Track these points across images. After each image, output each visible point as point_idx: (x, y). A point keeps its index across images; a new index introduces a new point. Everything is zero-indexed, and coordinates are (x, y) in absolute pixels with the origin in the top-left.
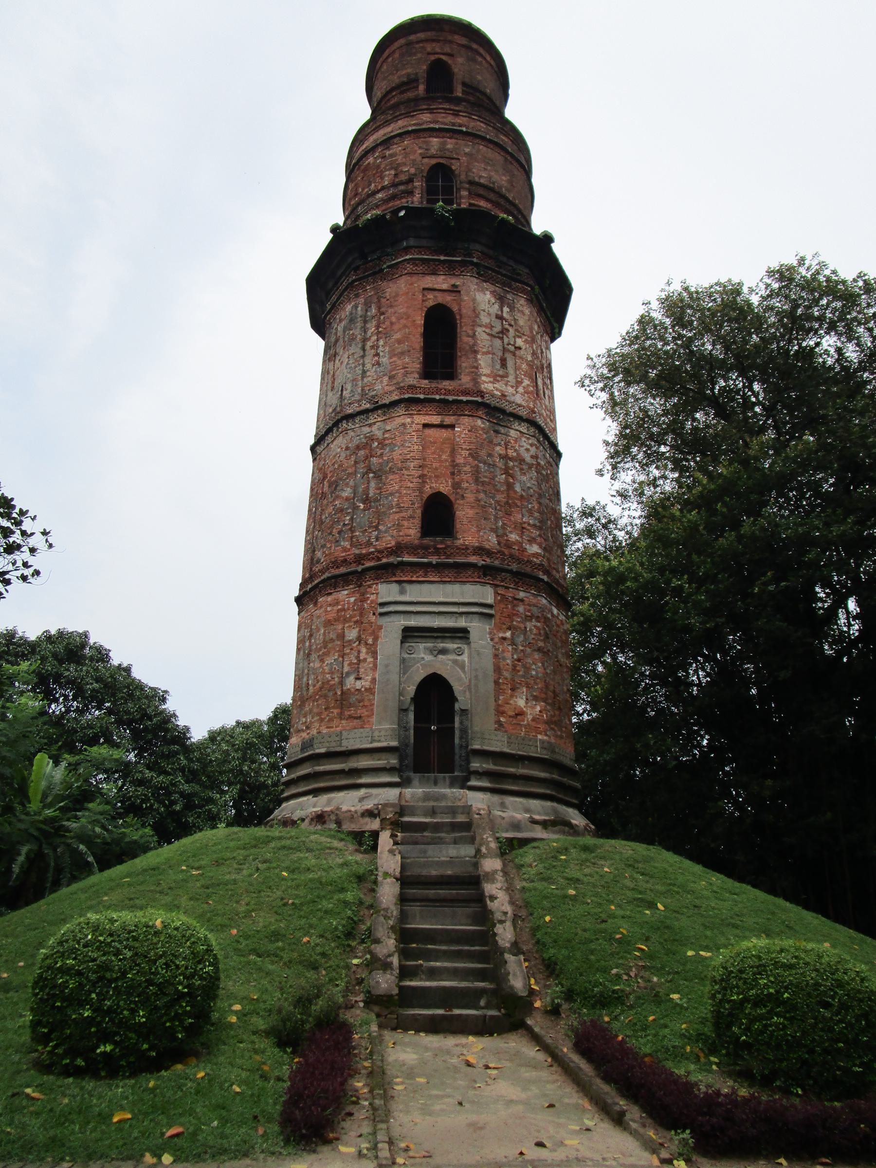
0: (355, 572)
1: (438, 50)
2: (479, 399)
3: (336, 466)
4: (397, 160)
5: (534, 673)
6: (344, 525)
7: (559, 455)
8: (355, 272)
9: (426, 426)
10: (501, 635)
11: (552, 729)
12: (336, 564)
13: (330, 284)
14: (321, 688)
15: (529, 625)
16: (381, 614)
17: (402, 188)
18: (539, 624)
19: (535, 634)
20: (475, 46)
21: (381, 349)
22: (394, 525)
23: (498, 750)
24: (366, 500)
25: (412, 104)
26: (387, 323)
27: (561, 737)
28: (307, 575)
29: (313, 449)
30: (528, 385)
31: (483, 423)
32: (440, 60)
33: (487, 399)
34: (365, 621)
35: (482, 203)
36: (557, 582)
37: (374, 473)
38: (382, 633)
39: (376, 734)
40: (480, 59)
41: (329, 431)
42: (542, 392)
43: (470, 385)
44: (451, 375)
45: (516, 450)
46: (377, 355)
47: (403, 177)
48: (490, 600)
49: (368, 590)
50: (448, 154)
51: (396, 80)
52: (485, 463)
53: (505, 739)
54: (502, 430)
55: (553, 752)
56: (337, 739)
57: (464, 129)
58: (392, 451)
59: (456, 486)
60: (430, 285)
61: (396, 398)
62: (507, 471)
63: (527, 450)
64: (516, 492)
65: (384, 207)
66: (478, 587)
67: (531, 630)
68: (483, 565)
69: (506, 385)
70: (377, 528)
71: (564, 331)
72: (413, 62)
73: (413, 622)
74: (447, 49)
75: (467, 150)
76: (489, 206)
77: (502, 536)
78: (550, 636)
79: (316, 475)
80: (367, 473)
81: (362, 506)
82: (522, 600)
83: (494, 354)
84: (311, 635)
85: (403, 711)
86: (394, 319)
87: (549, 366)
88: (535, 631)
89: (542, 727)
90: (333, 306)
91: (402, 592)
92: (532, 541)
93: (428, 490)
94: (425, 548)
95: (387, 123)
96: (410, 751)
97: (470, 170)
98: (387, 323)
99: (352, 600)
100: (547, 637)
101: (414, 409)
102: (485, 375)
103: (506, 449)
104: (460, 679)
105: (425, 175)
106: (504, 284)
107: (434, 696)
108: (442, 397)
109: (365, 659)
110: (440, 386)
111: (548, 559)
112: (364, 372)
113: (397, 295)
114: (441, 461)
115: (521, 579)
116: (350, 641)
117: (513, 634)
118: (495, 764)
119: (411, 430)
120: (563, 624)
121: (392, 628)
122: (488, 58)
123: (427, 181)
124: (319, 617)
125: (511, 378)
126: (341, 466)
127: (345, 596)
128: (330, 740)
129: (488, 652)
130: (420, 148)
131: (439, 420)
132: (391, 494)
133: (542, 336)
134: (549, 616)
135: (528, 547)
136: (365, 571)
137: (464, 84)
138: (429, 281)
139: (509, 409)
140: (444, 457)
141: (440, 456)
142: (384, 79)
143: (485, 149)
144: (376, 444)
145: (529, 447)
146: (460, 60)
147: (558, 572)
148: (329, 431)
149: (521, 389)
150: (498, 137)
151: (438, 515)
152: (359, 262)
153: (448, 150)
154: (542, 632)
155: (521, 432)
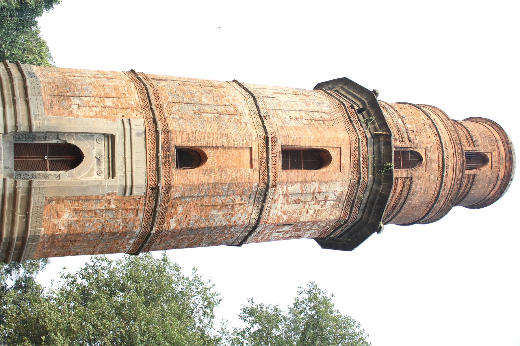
0: (151, 105)
1: (494, 159)
2: (270, 184)
3: (222, 94)
4: (423, 132)
5: (87, 225)
6: (183, 98)
7: (240, 245)
8: (350, 106)
9: (251, 149)
10: (112, 201)
11: (49, 240)
12: (156, 92)
13: (343, 92)
14: (71, 83)
15: (120, 220)
16: (123, 120)
17: (405, 135)
18: (121, 228)
19: (114, 225)
20: (499, 183)
21: (300, 121)
22: (183, 128)
23: (32, 200)
24: (200, 112)
25: (459, 142)
26: (317, 125)
27: (43, 247)
28: (149, 77)
29: (235, 81)
30: (283, 219)
31: (255, 187)
32: (488, 160)
33: (271, 190)
34: (118, 110)
35: (399, 187)
36: (152, 243)
37: (218, 117)
38: (109, 121)
39: (40, 117)
40: (491, 186)
41: (247, 90)
42: (280, 230)
43: (279, 179)
44: (285, 167)
45: (239, 210)
46: (297, 119)
47: (412, 136)
48: (135, 192)
49: (139, 113)
50: (428, 164)
51: (475, 133)
52: (228, 189)
53: (40, 205)
54: (252, 200)
55: (33, 240)
56: (37, 93)
57: (445, 175)
58: (233, 128)
59: (212, 170)
60: (342, 153)
61: (268, 131)
62: (224, 205)
63: (240, 218)
64: (210, 210)
65: (392, 124)
66: (144, 183)
67: (117, 222)
68: (159, 187)
69: (282, 203)
70: (182, 118)
71: (325, 249)
72: (486, 143)
73: (119, 142)
74: (495, 165)
75: (432, 177)
76: (398, 192)
78: (114, 237)
79: (217, 83)
80: (218, 113)
81: (196, 109)
82: (137, 215)
83: (302, 194)
84: (108, 78)
85: (58, 134)
86: (320, 129)
87: (300, 237)
88: (116, 225)
89: (50, 232)
90: (329, 94)
91: (138, 134)
92: (178, 222)
93: (207, 152)
94: (169, 149)
95: (446, 126)
96: (29, 141)
97: (419, 179)
98: (317, 125)
99: (132, 103)
100: (113, 234)
101: (263, 142)
102: (287, 188)
104: (80, 174)
105: (415, 150)
106: (348, 201)
107: (69, 156)
108: (270, 160)
109: (92, 111)
110: (277, 158)
111: (167, 235)
112: (285, 111)
113: (335, 131)
114: (228, 159)
115: (151, 215)
116: (104, 101)
117: (113, 210)
118: (21, 198)
119: (248, 140)
120: (123, 248)
121: (113, 127)
122: (493, 192)
123: (411, 151)
124: (120, 82)
125: (286, 207)
126: (223, 97)
127: (135, 98)
128: (36, 88)
129: (100, 192)
130: (431, 147)
131: (255, 158)
132: (204, 127)
133: (318, 230)
134: (128, 237)
135: (174, 219)
136: (152, 109)
137: (474, 176)
138: (346, 152)
139: (266, 205)
140: (231, 161)
141: (231, 159)
142: (475, 128)
143: (434, 188)
144: (238, 118)
145: (242, 220)
146: (489, 174)
147: (160, 243)
148: (247, 90)
149: (280, 214)
150: (442, 197)
151: (190, 157)
152: (356, 108)
153: (431, 164)
154: (116, 230)
155: (251, 214)
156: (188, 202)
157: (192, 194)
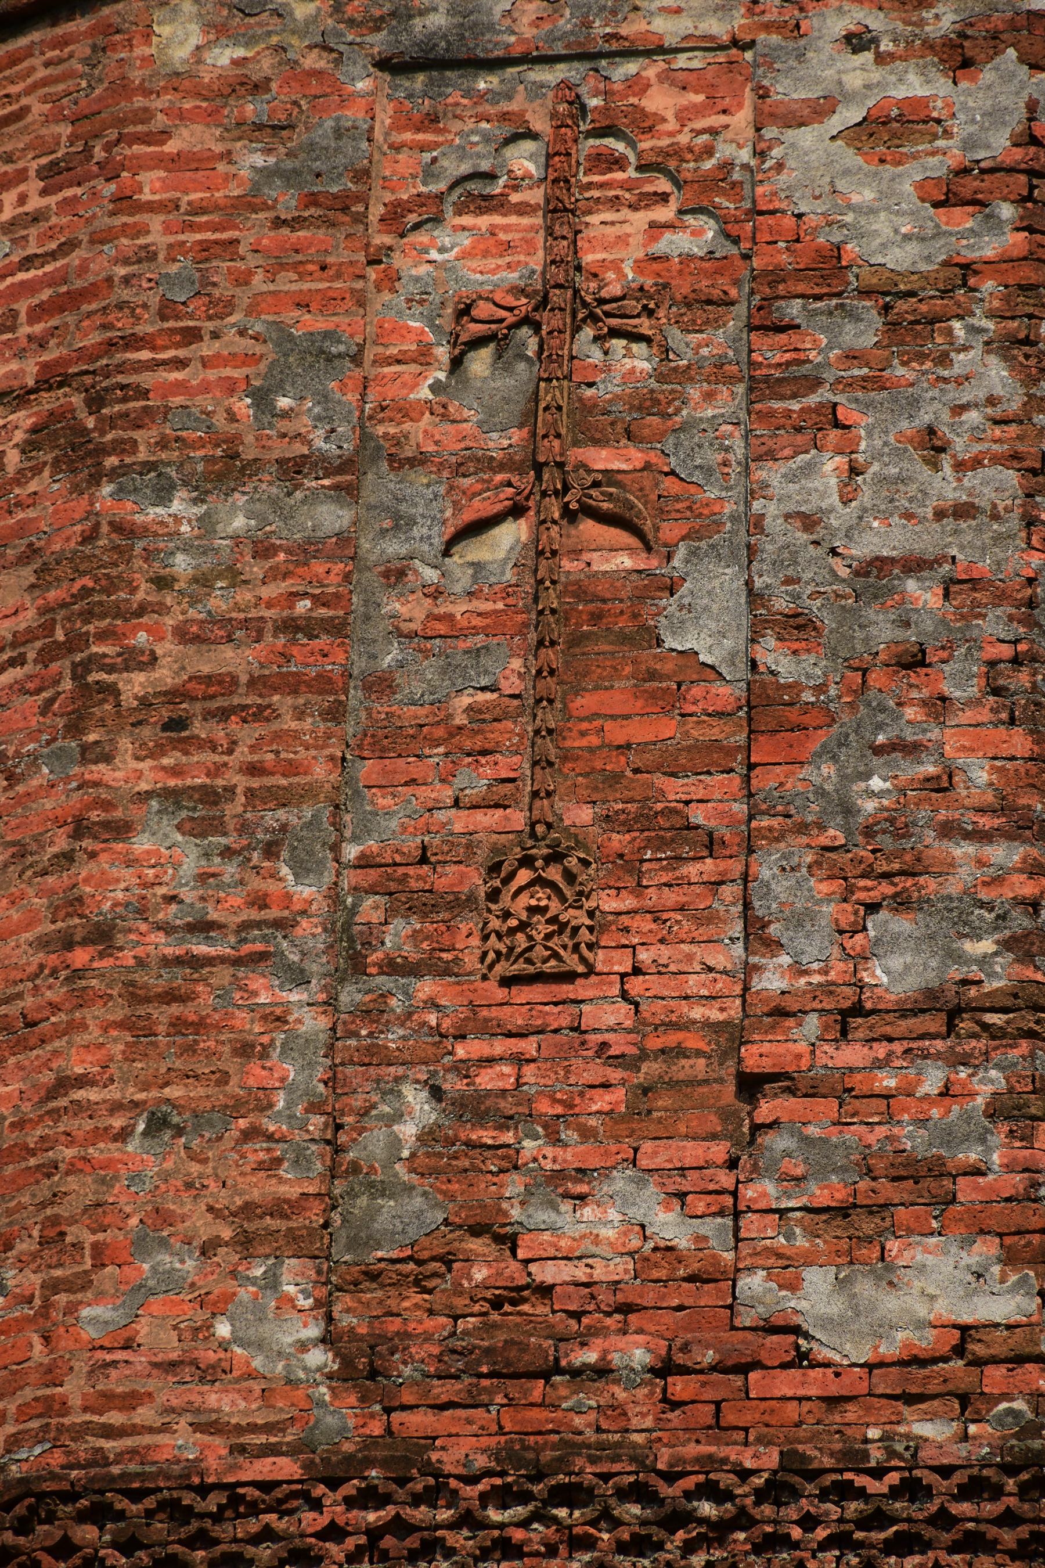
63: (887, 131)
77: (427, 1267)
103: (561, 212)
145: (915, 84)
156: (474, 1108)
157: (290, 1077)
